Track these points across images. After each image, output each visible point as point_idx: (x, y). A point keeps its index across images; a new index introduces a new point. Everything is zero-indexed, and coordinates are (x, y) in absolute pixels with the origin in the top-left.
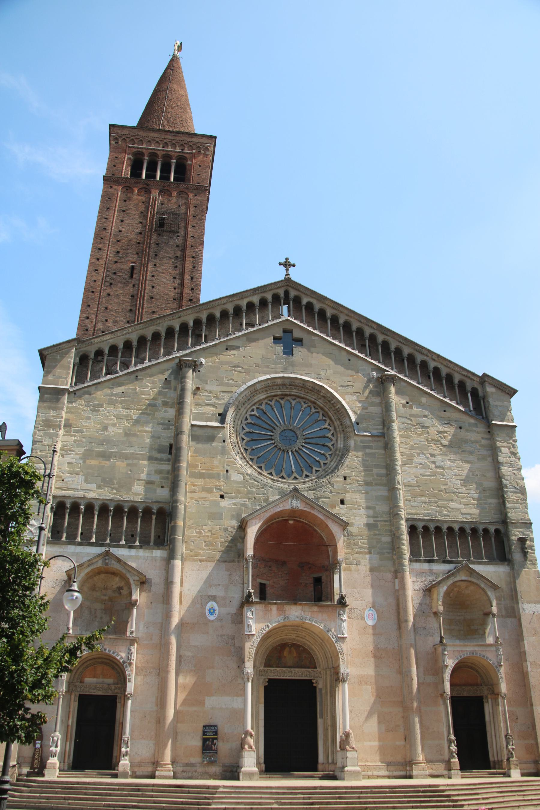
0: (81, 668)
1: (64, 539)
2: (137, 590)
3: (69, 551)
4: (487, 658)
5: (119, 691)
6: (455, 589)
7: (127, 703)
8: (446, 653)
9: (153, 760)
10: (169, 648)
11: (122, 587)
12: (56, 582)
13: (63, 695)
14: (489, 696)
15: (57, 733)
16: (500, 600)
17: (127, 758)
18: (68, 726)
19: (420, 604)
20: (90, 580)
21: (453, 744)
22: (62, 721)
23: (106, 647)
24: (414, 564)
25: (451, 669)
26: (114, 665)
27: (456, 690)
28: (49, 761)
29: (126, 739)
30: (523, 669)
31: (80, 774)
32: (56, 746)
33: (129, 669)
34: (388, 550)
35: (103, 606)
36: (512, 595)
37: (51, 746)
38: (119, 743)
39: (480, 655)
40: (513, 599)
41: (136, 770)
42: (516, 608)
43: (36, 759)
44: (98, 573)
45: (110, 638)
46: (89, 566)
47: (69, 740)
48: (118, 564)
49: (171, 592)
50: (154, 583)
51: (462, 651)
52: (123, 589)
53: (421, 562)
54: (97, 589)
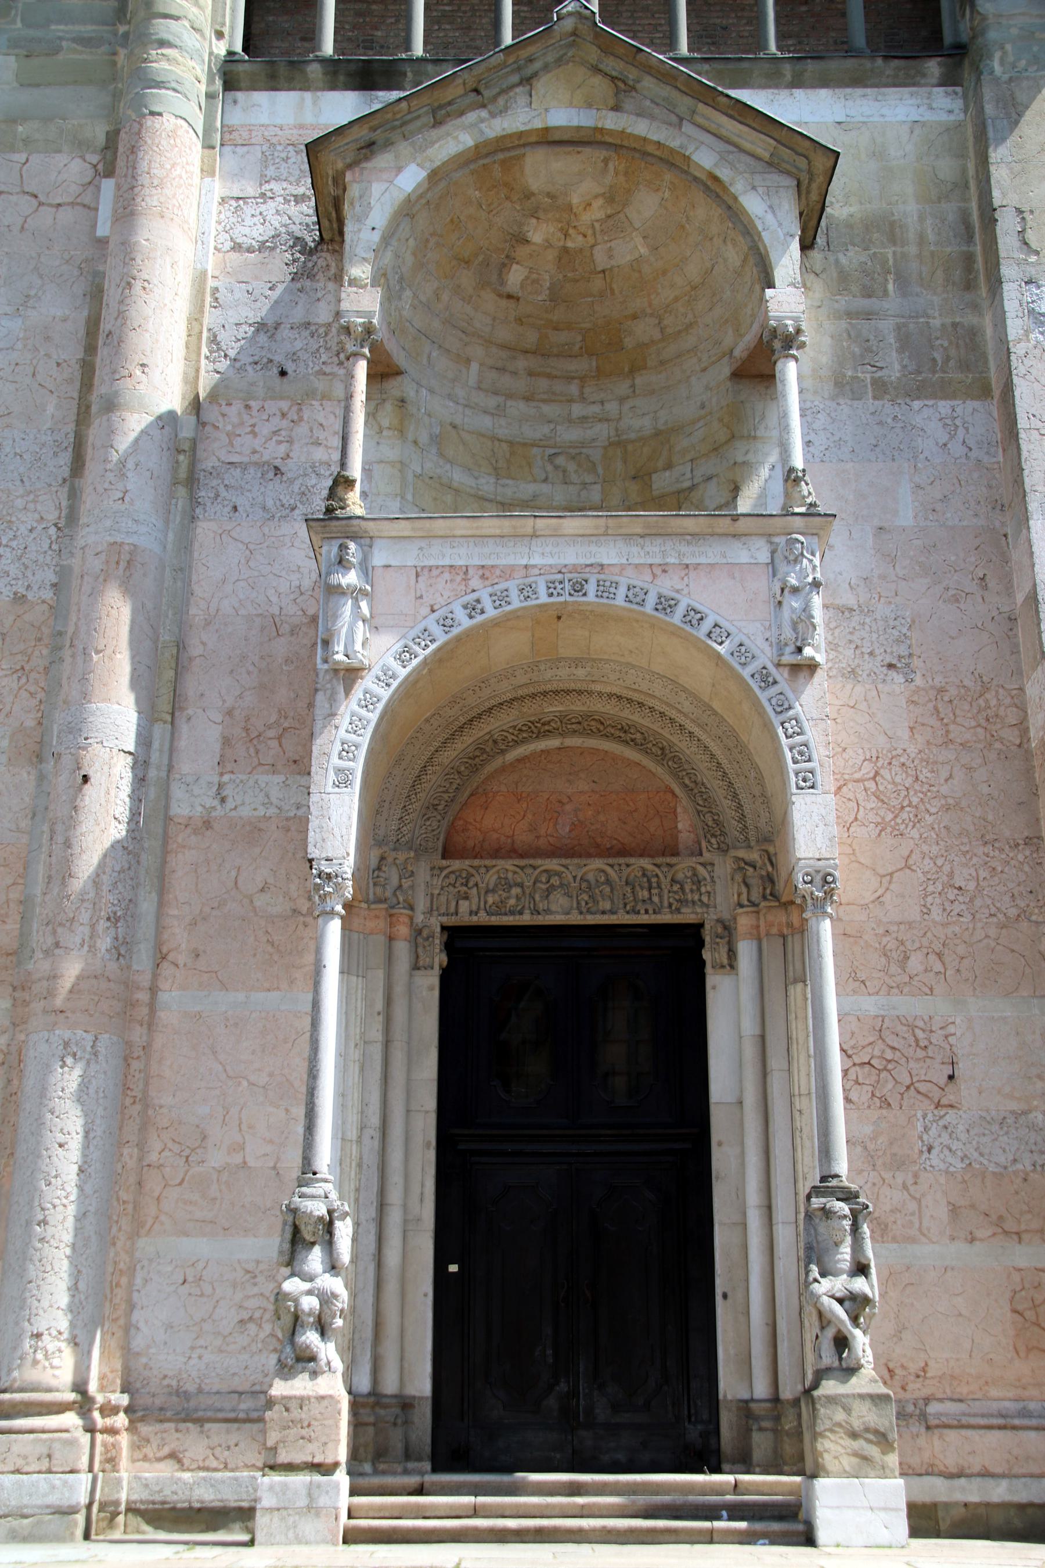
4: (694, 616)
6: (538, 233)
8: (351, 578)
14: (744, 922)
16: (868, 293)
19: (261, 327)
21: (315, 1258)
24: (262, 97)
25: (385, 694)
27: (491, 878)
30: (1022, 727)
34: (88, 29)
36: (969, 259)
39: (635, 595)
40: (969, 285)
42: (989, 332)
51: (485, 572)
53: (305, 86)
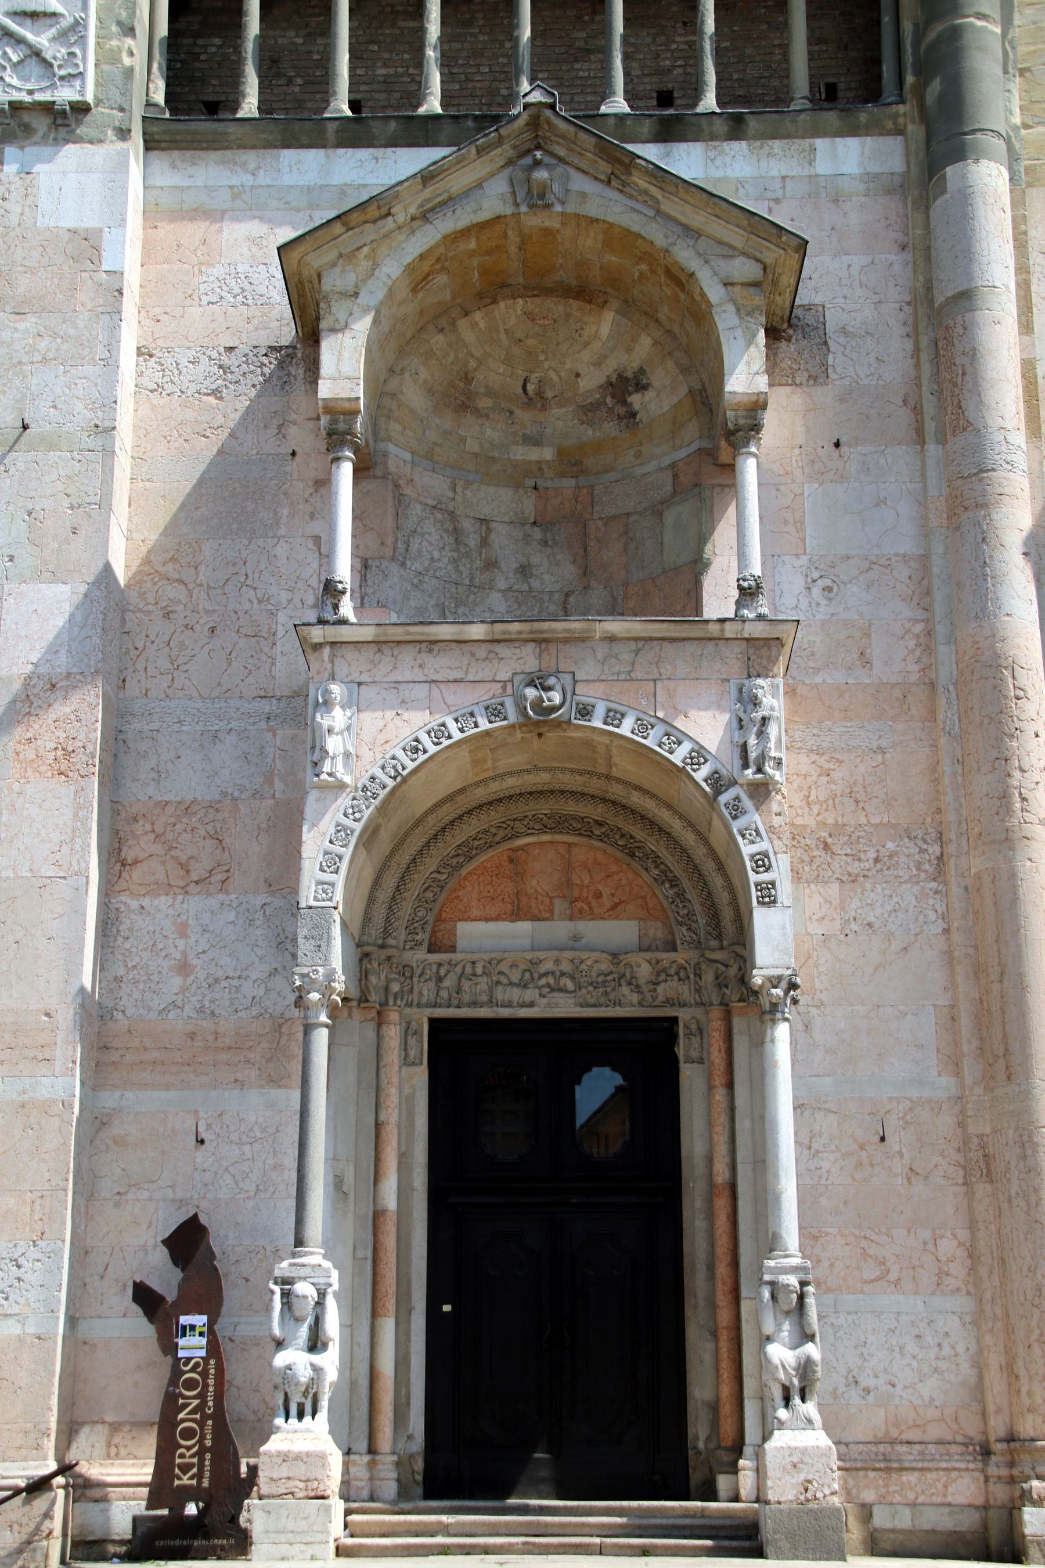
0: (431, 864)
1: (250, 105)
2: (751, 340)
3: (289, 179)
5: (685, 991)
7: (760, 1043)
9: (973, 1430)
10: (998, 688)
11: (642, 371)
12: (225, 360)
13: (333, 1012)
15: (315, 1257)
17: (810, 1408)
18: (378, 1216)
20: (438, 341)
22: (337, 1184)
23: (586, 694)
26: (640, 834)
28: (274, 1444)
29: (792, 1280)
31: (494, 1531)
32: (316, 1344)
33: (755, 818)
35: (529, 505)
37: (280, 1344)
38: (724, 1317)
41: (869, 1496)
43: (188, 1434)
44: (480, 296)
45: (612, 639)
46: (424, 216)
47: (391, 1304)
48: (610, 193)
49: (973, 354)
50: (844, 331)
52: (641, 387)
54: (484, 403)
